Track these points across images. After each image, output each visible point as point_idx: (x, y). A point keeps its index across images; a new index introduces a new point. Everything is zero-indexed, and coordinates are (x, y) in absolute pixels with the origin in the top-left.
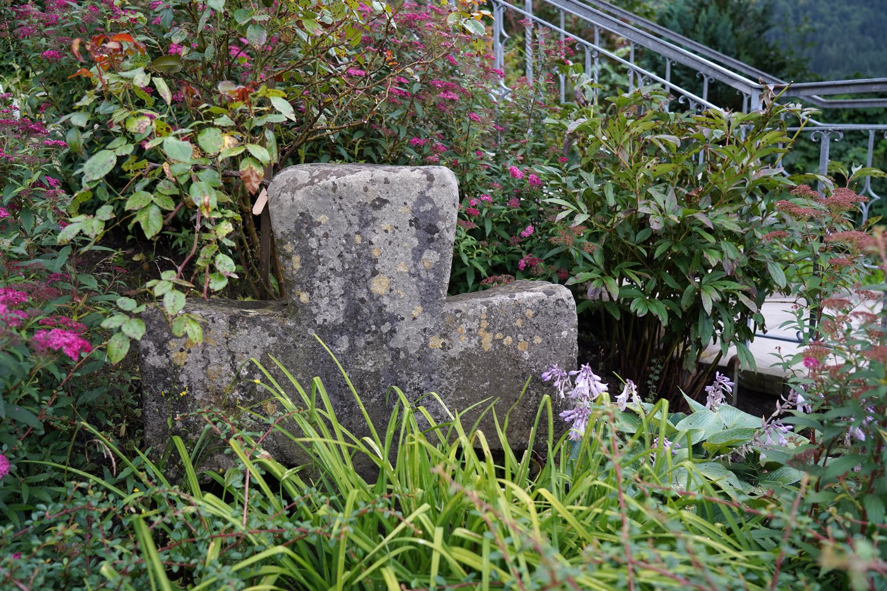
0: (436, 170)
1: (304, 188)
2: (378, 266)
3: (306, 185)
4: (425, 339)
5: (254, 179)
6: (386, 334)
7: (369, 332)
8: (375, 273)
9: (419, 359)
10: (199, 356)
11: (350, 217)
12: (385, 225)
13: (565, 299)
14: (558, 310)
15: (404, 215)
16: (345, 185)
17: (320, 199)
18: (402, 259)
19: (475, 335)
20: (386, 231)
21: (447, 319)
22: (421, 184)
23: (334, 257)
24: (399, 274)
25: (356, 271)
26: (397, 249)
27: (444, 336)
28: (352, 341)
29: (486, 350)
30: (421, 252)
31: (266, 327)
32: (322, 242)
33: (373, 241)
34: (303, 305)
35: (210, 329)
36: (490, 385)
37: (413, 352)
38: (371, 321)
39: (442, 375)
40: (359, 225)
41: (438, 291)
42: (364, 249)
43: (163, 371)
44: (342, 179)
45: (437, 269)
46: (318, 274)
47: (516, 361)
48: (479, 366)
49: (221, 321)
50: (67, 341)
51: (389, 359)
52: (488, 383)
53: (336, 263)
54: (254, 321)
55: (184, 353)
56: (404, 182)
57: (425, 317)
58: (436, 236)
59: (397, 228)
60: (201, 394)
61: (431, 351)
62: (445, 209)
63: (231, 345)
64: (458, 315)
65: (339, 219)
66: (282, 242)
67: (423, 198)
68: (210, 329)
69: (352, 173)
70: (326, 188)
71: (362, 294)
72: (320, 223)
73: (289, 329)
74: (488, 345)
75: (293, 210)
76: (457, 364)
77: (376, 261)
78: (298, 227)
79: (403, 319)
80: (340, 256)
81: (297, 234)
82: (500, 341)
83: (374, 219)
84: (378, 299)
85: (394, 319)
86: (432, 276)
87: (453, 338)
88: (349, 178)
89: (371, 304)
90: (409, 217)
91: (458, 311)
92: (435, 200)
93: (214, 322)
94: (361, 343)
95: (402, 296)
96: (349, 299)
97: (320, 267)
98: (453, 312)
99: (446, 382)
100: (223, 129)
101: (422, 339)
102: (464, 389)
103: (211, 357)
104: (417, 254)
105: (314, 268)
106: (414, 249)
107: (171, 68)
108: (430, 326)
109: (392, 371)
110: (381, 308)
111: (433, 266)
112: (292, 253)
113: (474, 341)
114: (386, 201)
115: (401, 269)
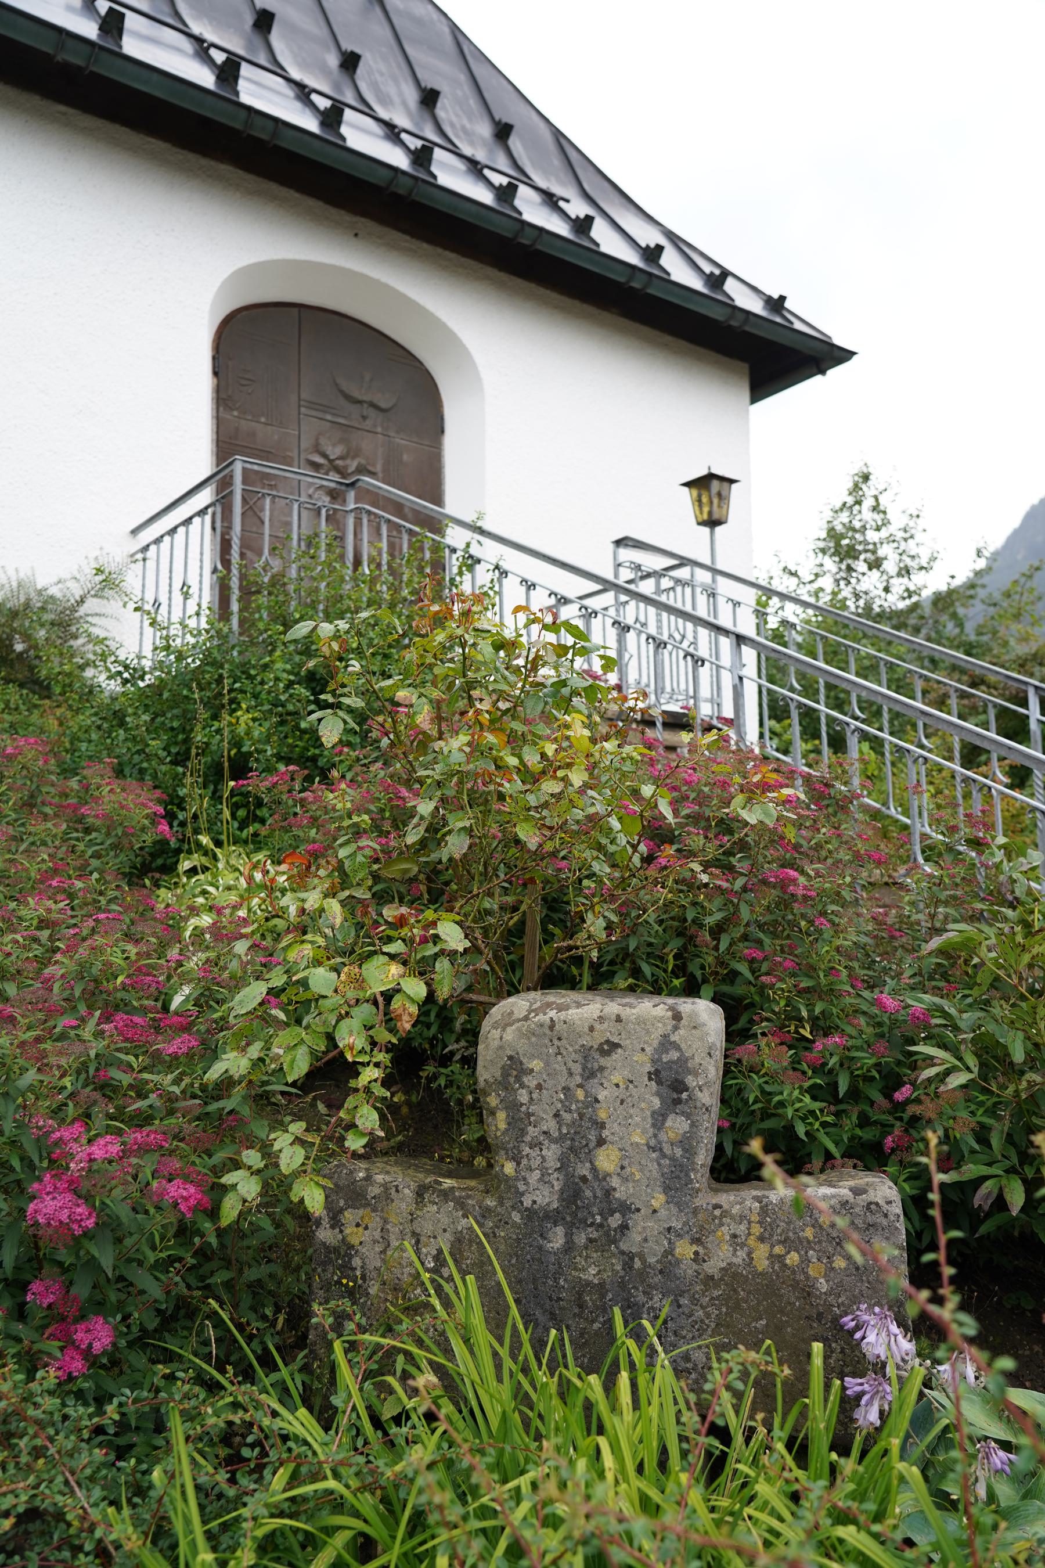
0: (687, 1006)
1: (517, 1025)
2: (605, 1133)
3: (519, 1020)
4: (670, 1243)
5: (406, 1018)
6: (615, 1230)
7: (592, 1224)
8: (601, 1142)
9: (661, 1272)
10: (377, 1235)
11: (571, 1064)
12: (616, 1078)
13: (881, 1202)
14: (870, 1219)
15: (642, 1065)
16: (565, 1022)
17: (533, 1039)
18: (637, 1125)
19: (743, 1245)
20: (617, 1085)
21: (700, 1216)
22: (665, 1025)
23: (548, 1116)
24: (633, 1147)
25: (577, 1138)
26: (632, 1111)
27: (696, 1241)
28: (569, 1235)
29: (760, 1269)
30: (664, 1117)
31: (461, 1204)
32: (535, 1096)
33: (600, 1097)
34: (507, 1179)
35: (392, 1201)
36: (767, 1325)
37: (652, 1260)
38: (595, 1210)
39: (694, 1301)
40: (582, 1075)
41: (687, 1175)
42: (587, 1108)
43: (336, 1250)
44: (563, 1015)
45: (687, 1144)
46: (528, 1139)
47: (807, 1292)
48: (749, 1292)
49: (407, 1191)
50: (185, 1194)
51: (619, 1268)
52: (764, 1322)
53: (550, 1125)
54: (446, 1195)
55: (360, 1229)
56: (641, 1021)
57: (669, 1209)
58: (684, 1095)
59: (631, 1082)
60: (376, 1288)
61: (678, 1262)
62: (697, 1060)
63: (415, 1224)
64: (717, 1212)
65: (556, 1066)
66: (486, 1094)
67: (666, 1044)
68: (392, 1201)
69: (579, 1005)
70: (542, 1025)
71: (584, 1170)
72: (532, 1070)
73: (488, 1210)
74: (762, 1263)
75: (500, 1052)
76: (717, 1286)
77: (602, 1126)
78: (505, 1074)
79: (638, 1210)
80: (556, 1115)
81: (503, 1084)
82: (780, 1258)
83: (602, 1069)
84: (604, 1179)
85: (625, 1209)
86: (678, 1152)
87: (709, 1245)
88: (573, 1013)
89: (596, 1184)
90: (648, 1067)
91: (717, 1206)
92: (683, 1046)
93: (397, 1191)
94: (581, 1239)
95: (638, 1177)
96: (566, 1175)
97: (530, 1129)
98: (710, 1207)
99: (701, 1313)
100: (392, 957)
101: (665, 1243)
102: (728, 1327)
103: (392, 1237)
104: (659, 1119)
105: (523, 1130)
106: (653, 1113)
107: (406, 871)
108: (677, 1224)
109: (622, 1285)
110: (609, 1192)
111: (680, 1138)
112: (497, 1108)
113: (742, 1254)
114: (617, 1046)
115: (637, 1139)
